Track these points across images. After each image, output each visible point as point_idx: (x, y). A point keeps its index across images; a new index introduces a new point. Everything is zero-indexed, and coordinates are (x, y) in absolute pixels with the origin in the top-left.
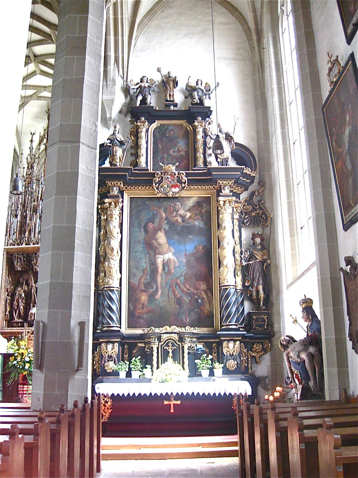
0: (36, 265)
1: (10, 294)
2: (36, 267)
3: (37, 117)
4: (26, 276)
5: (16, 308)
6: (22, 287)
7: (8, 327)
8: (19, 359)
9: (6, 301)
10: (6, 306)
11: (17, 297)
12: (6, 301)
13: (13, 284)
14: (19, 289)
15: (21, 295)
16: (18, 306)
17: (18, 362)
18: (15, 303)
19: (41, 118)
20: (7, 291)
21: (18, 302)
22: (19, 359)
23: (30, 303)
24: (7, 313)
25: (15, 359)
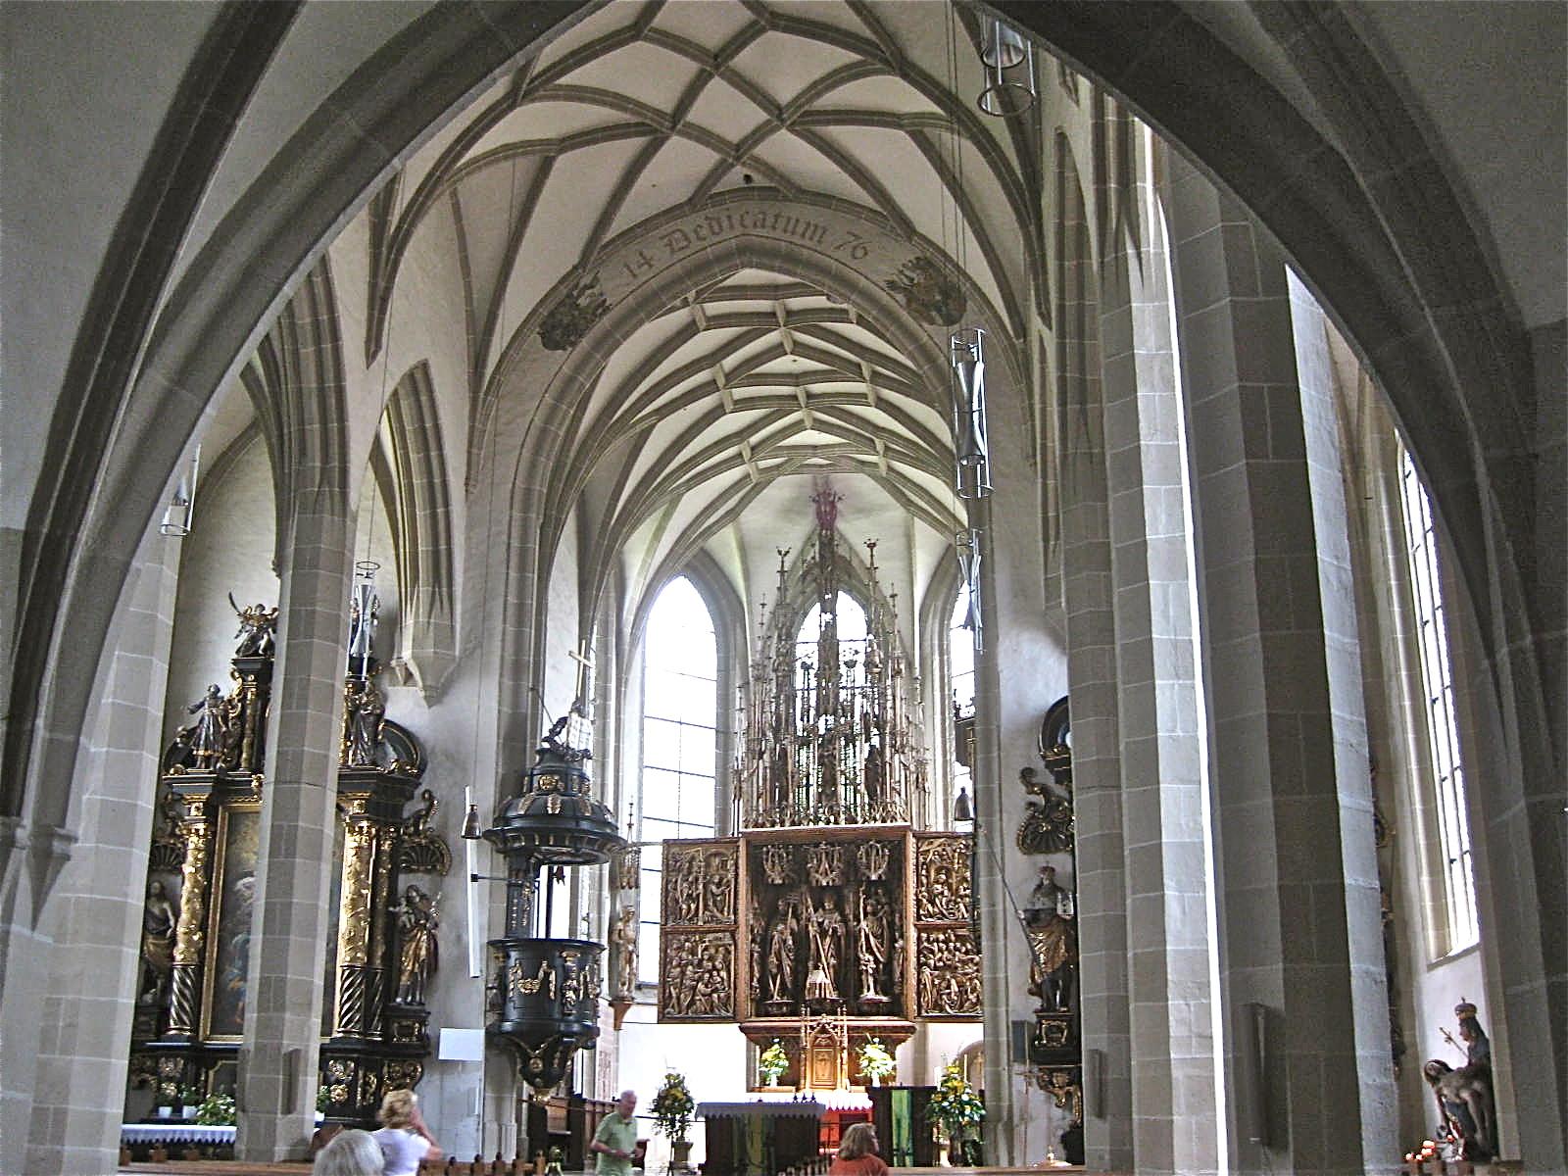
0: (817, 872)
1: (758, 940)
2: (817, 876)
3: (789, 511)
4: (793, 899)
5: (775, 971)
6: (784, 922)
7: (757, 1016)
8: (951, 1098)
9: (752, 956)
10: (751, 967)
11: (775, 947)
12: (752, 956)
13: (763, 916)
14: (781, 927)
15: (785, 942)
16: (780, 967)
17: (951, 1103)
18: (773, 959)
19: (798, 513)
20: (752, 931)
21: (780, 960)
22: (951, 1098)
23: (807, 960)
24: (755, 983)
25: (945, 1099)
